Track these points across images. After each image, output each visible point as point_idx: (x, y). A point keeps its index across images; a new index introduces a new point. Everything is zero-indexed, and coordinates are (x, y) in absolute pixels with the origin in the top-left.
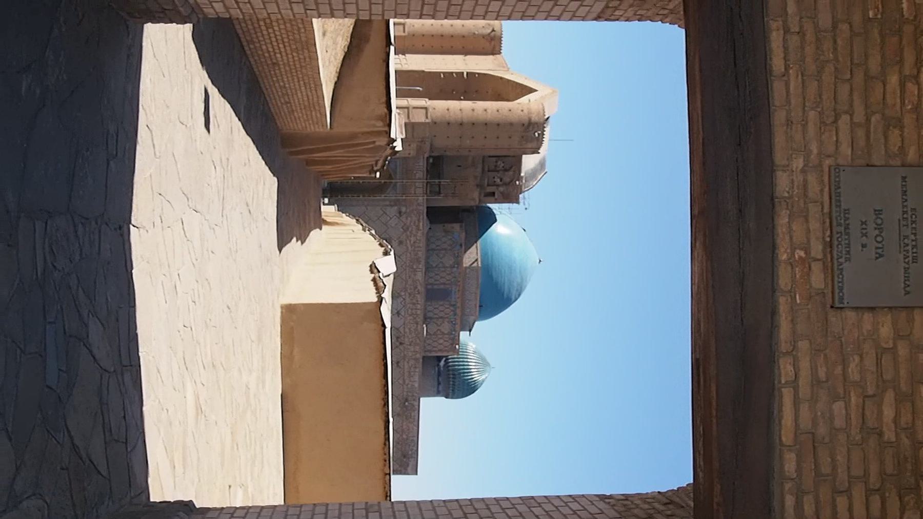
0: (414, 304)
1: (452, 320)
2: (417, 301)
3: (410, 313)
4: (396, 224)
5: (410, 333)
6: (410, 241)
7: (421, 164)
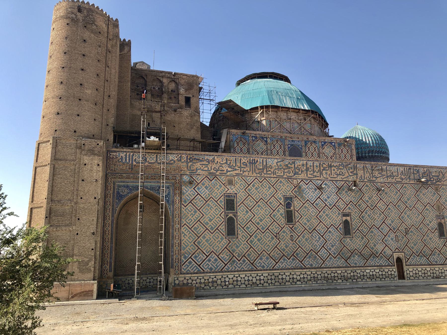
0: (307, 169)
1: (320, 144)
2: (303, 165)
3: (318, 174)
4: (206, 188)
5: (342, 174)
6: (228, 171)
7: (123, 155)
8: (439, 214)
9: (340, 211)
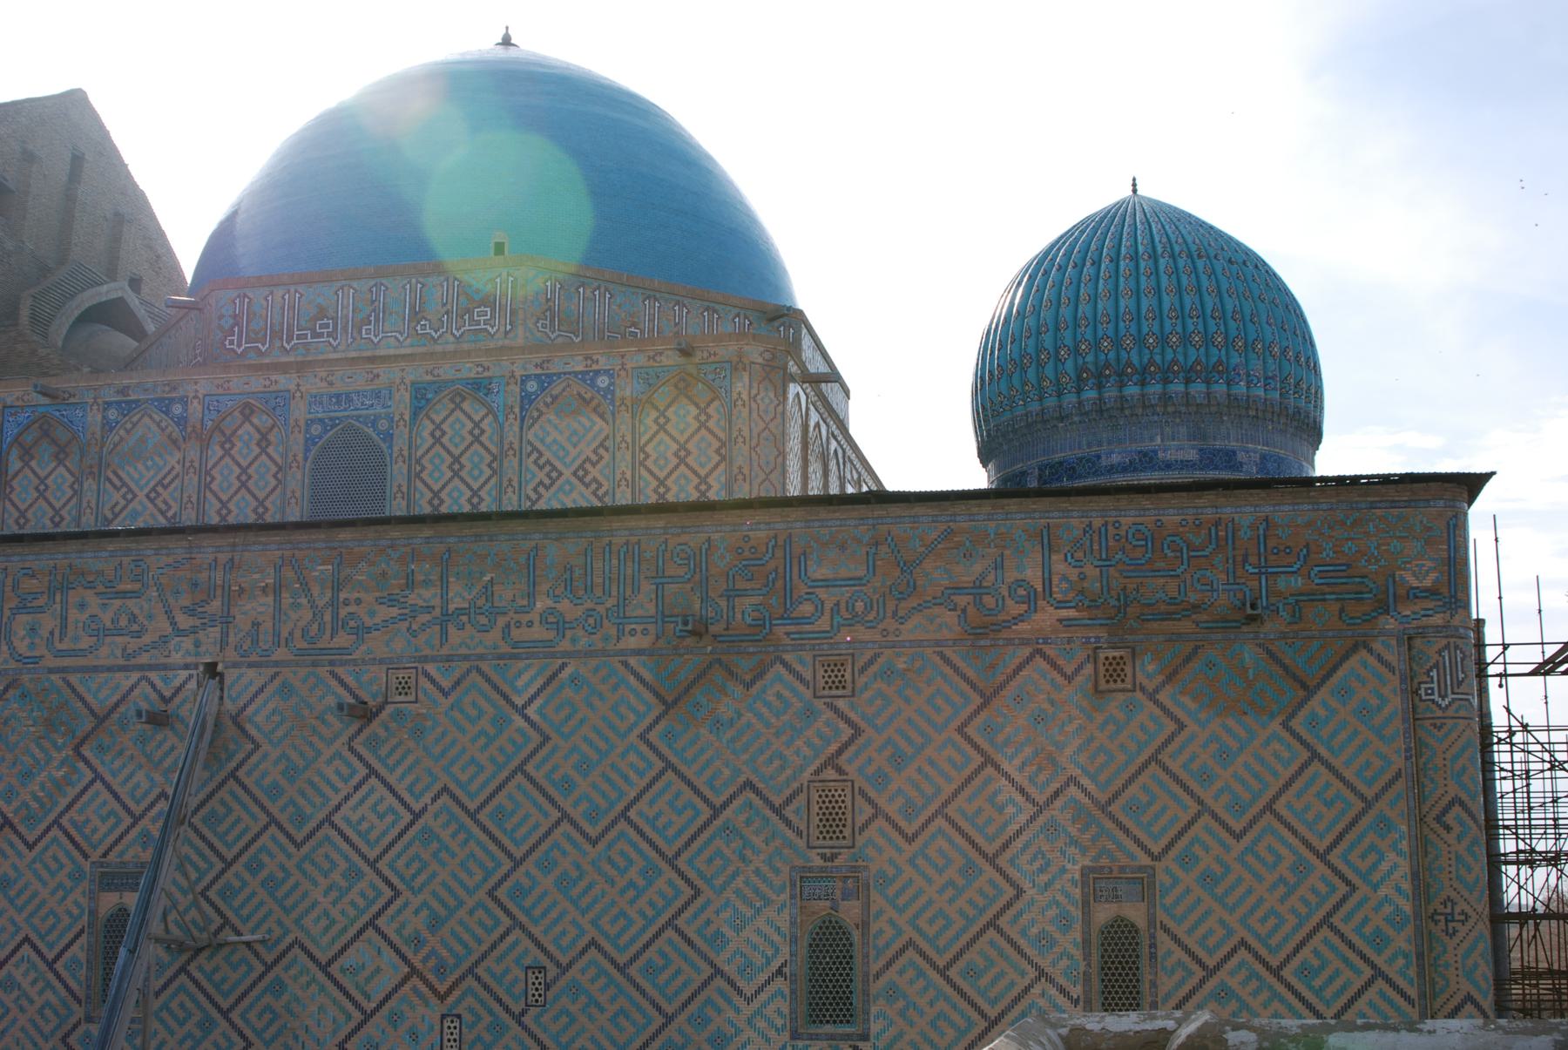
8: (819, 862)
9: (86, 856)
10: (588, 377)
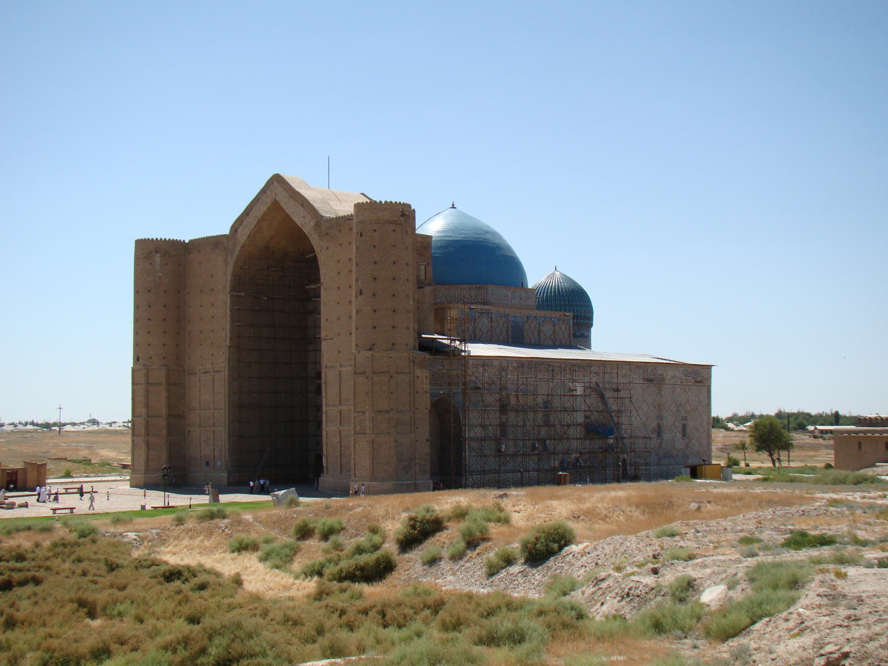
10: (551, 318)
